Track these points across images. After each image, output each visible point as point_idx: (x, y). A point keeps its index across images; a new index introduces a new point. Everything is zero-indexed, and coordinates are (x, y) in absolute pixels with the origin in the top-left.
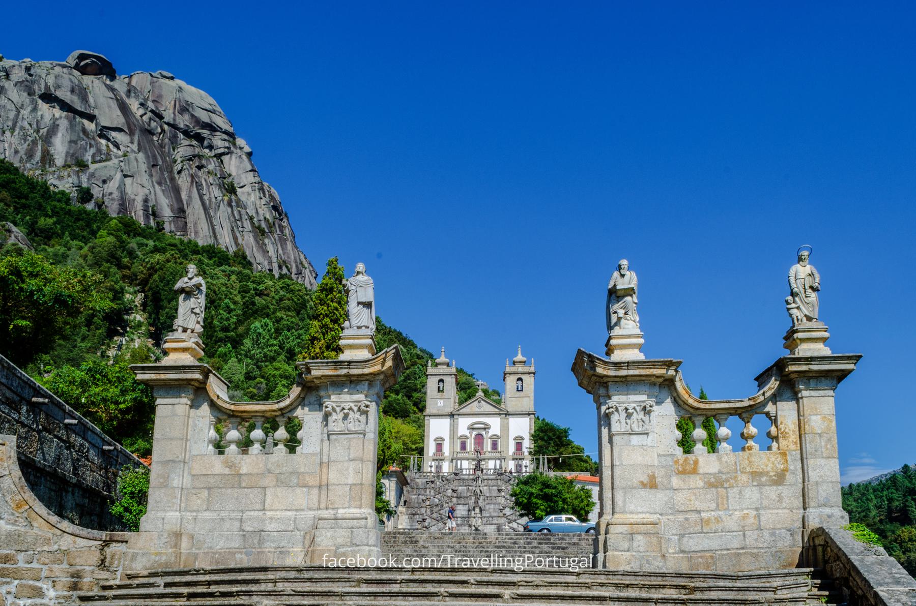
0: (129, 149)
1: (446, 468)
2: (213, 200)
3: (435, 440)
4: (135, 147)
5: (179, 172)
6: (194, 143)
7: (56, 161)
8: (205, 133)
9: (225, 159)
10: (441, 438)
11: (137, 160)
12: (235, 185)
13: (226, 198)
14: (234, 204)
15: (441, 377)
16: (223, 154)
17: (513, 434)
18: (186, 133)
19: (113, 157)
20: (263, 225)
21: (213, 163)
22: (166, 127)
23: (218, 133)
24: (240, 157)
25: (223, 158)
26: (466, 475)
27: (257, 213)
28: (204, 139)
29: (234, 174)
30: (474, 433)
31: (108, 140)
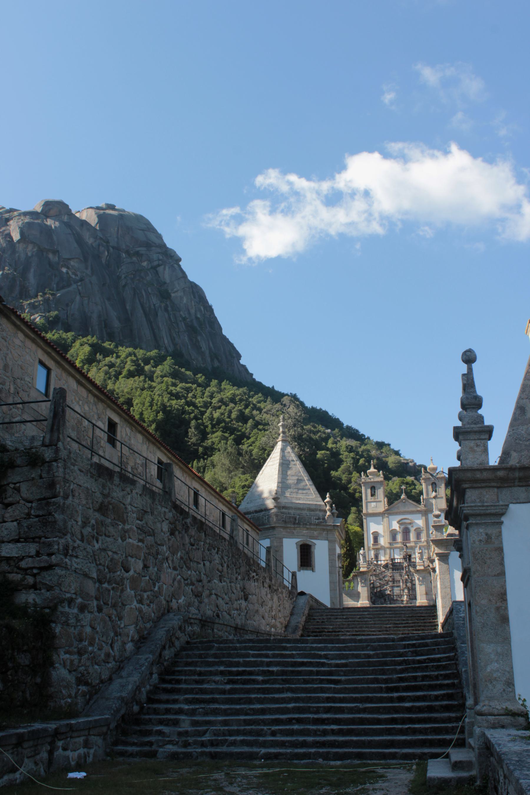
0: (84, 274)
1: (383, 559)
2: (152, 307)
3: (373, 533)
4: (89, 272)
5: (124, 286)
6: (134, 259)
7: (30, 292)
8: (142, 250)
9: (160, 269)
11: (91, 282)
12: (170, 291)
13: (163, 305)
14: (169, 309)
15: (373, 485)
16: (159, 265)
18: (127, 252)
19: (72, 282)
20: (195, 324)
21: (150, 275)
22: (111, 249)
23: (153, 248)
24: (172, 266)
25: (158, 269)
26: (398, 563)
27: (189, 313)
28: (142, 255)
29: (168, 281)
30: (402, 527)
31: (68, 268)
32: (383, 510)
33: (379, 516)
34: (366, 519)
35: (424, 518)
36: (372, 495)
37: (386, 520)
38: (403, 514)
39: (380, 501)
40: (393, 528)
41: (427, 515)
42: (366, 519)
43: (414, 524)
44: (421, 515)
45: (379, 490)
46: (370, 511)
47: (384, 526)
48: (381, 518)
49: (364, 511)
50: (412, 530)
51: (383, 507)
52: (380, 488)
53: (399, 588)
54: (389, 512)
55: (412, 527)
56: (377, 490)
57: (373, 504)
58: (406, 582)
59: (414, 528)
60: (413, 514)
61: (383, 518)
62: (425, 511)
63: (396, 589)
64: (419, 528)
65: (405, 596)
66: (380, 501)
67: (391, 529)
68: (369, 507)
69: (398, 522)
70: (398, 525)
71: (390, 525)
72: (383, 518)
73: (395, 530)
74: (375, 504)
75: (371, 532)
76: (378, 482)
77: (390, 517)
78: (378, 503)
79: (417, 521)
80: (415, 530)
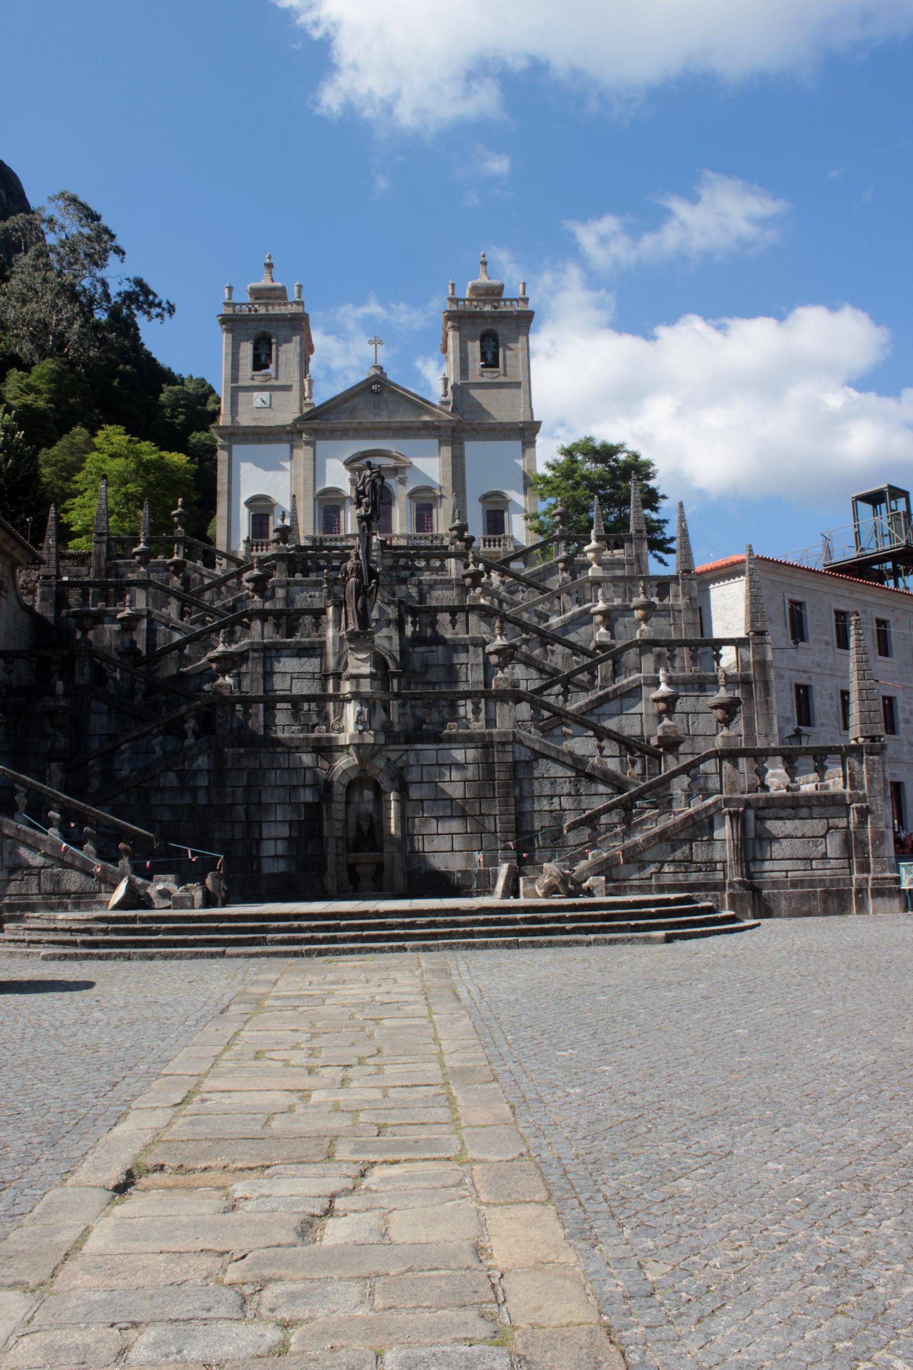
3: (250, 503)
10: (265, 498)
15: (263, 328)
17: (474, 491)
32: (298, 415)
33: (279, 441)
34: (229, 449)
35: (447, 451)
36: (259, 364)
37: (303, 453)
38: (374, 437)
39: (288, 388)
40: (329, 484)
41: (462, 444)
42: (229, 449)
43: (408, 473)
44: (435, 442)
45: (285, 347)
46: (245, 420)
47: (294, 478)
48: (286, 447)
49: (224, 420)
50: (401, 493)
51: (297, 409)
52: (288, 340)
53: (312, 665)
54: (315, 424)
55: (402, 482)
56: (278, 345)
57: (259, 398)
58: (361, 591)
59: (409, 488)
60: (406, 437)
61: (292, 448)
62: (453, 429)
63: (287, 664)
64: (429, 489)
65: (351, 711)
66: (288, 388)
67: (319, 489)
68: (241, 408)
69: (348, 464)
70: (348, 475)
71: (317, 471)
72: (292, 448)
73: (337, 491)
74: (265, 395)
75: (245, 496)
76: (282, 318)
77: (320, 444)
78: (277, 395)
79: (419, 463)
80: (411, 495)
